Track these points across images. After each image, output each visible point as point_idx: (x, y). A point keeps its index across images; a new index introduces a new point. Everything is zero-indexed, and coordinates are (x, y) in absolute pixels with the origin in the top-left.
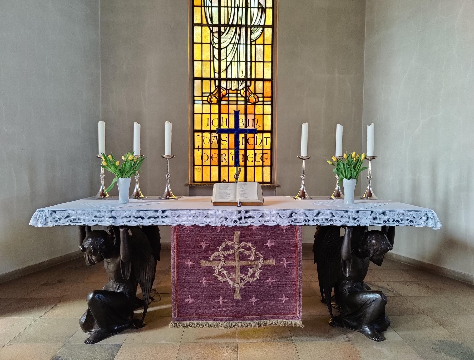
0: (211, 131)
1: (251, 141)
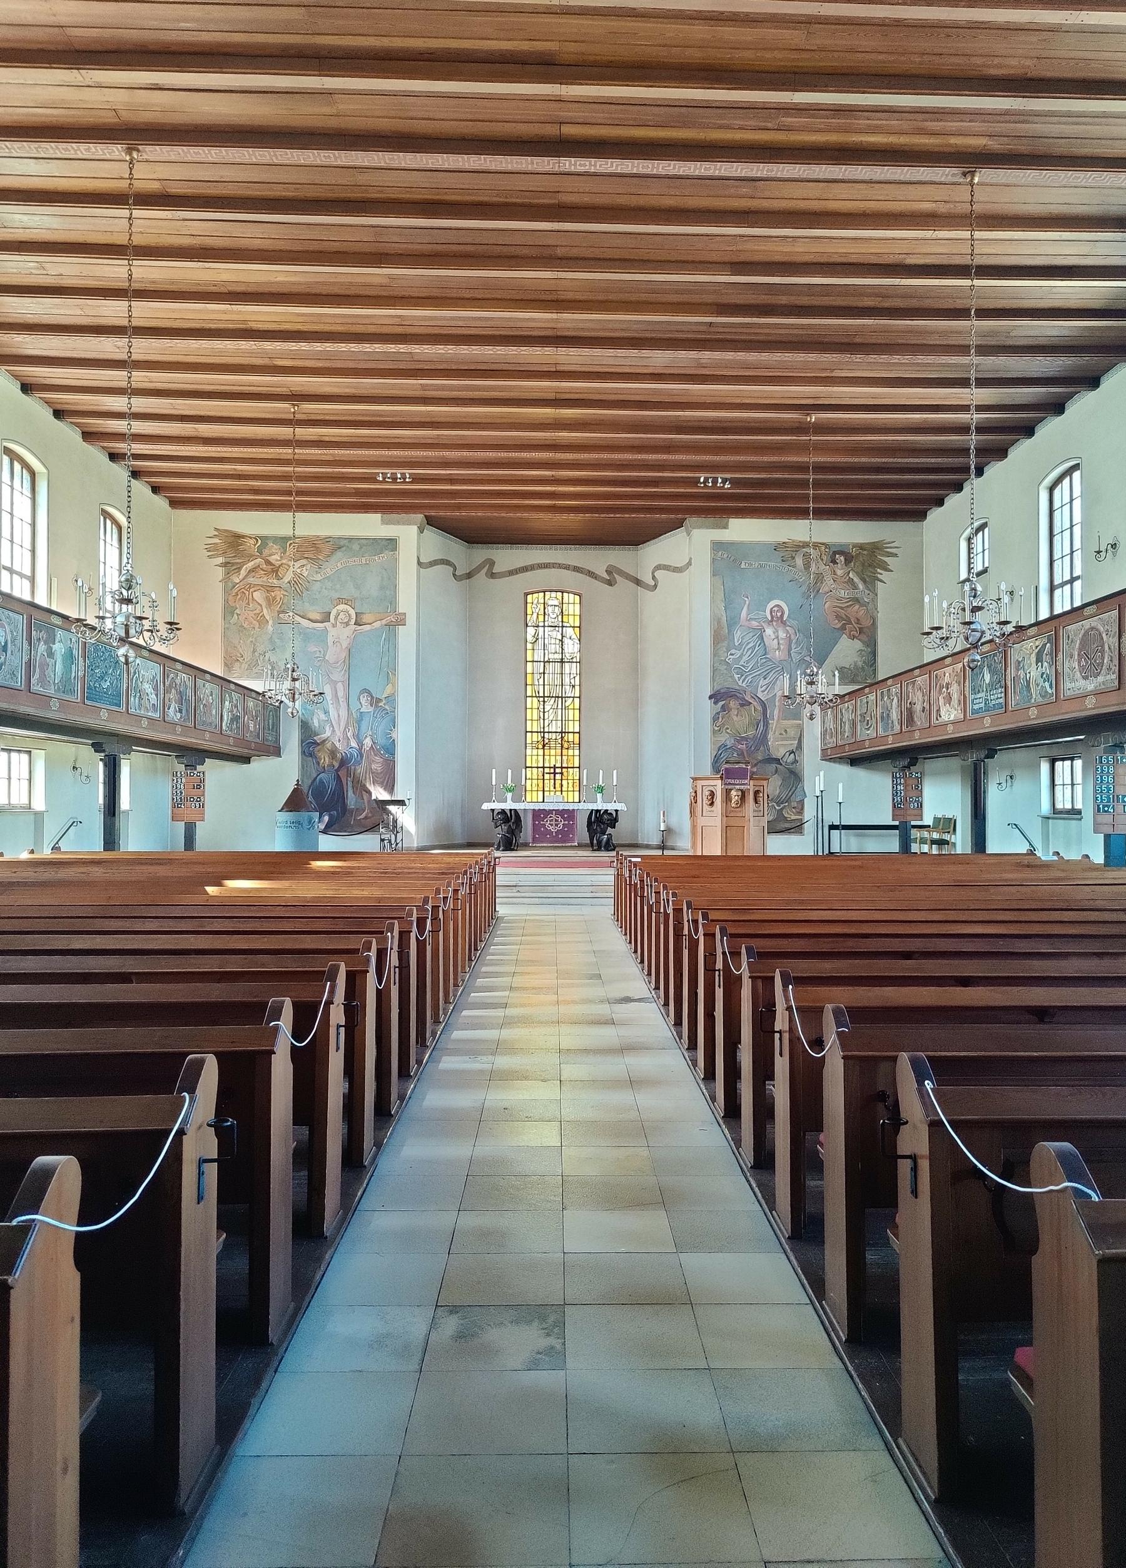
0: (538, 768)
1: (565, 774)
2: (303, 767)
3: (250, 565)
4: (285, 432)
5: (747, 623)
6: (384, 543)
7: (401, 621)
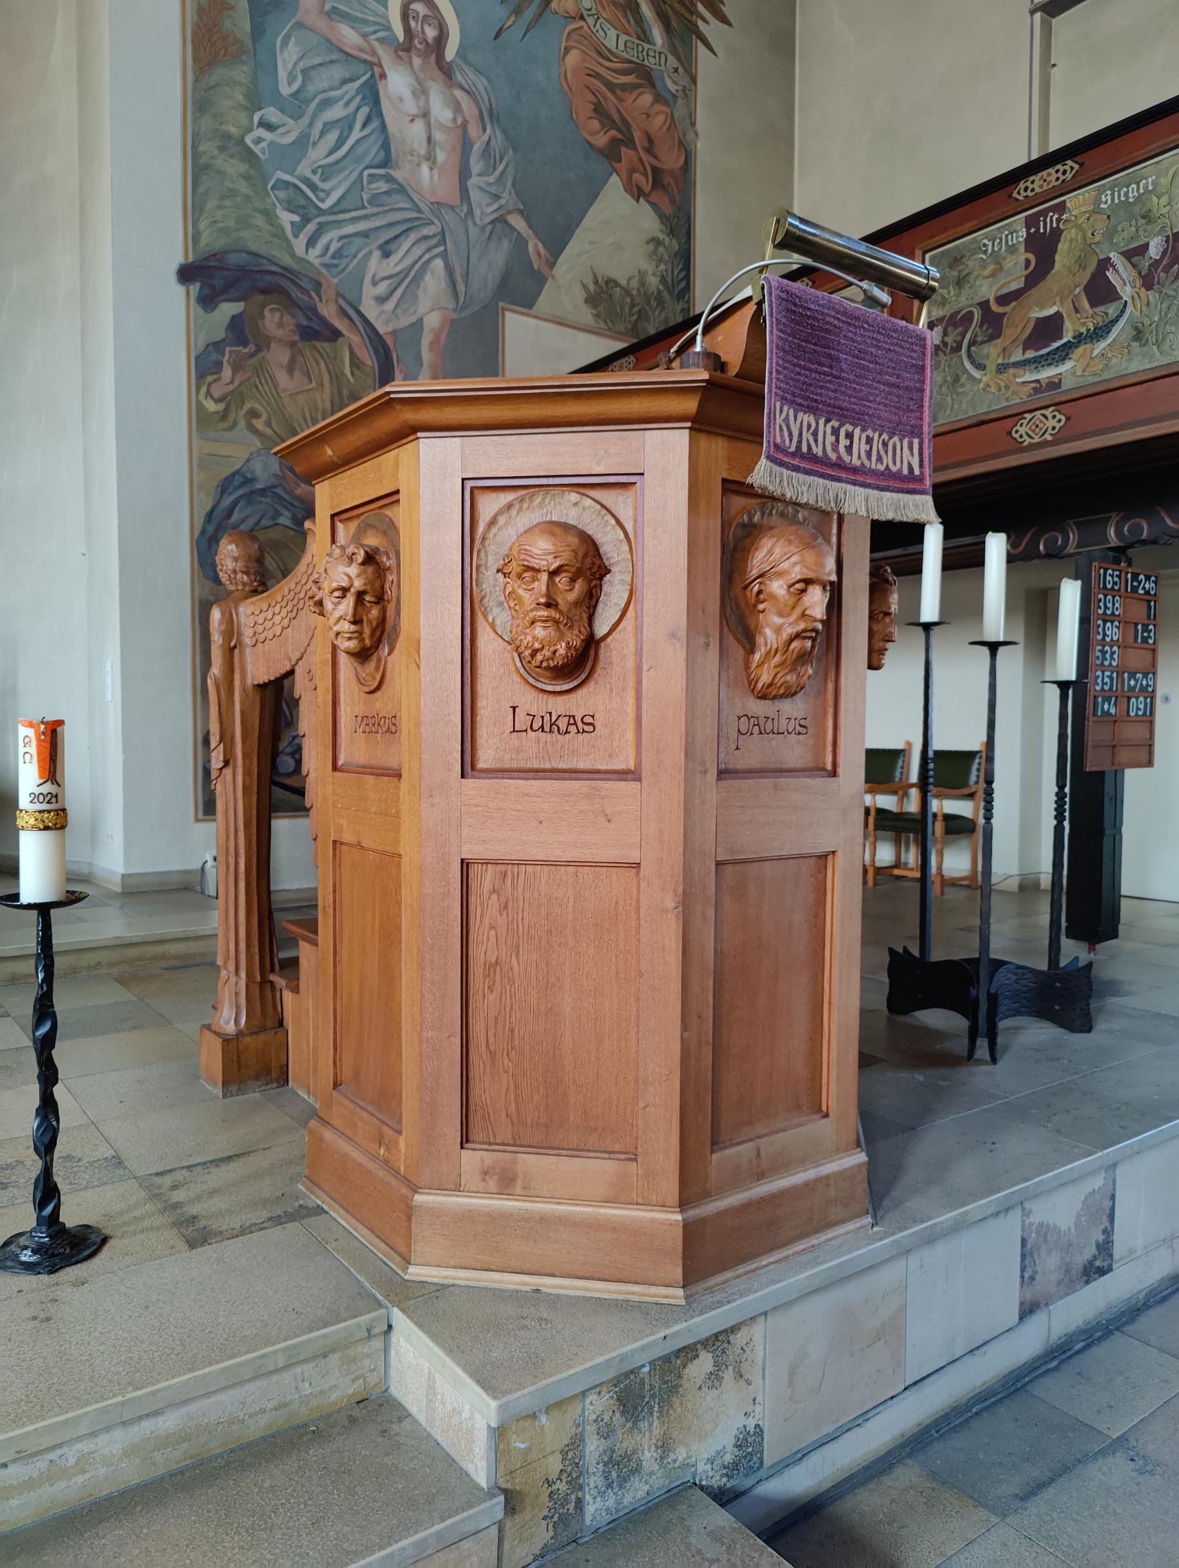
5: (322, 24)
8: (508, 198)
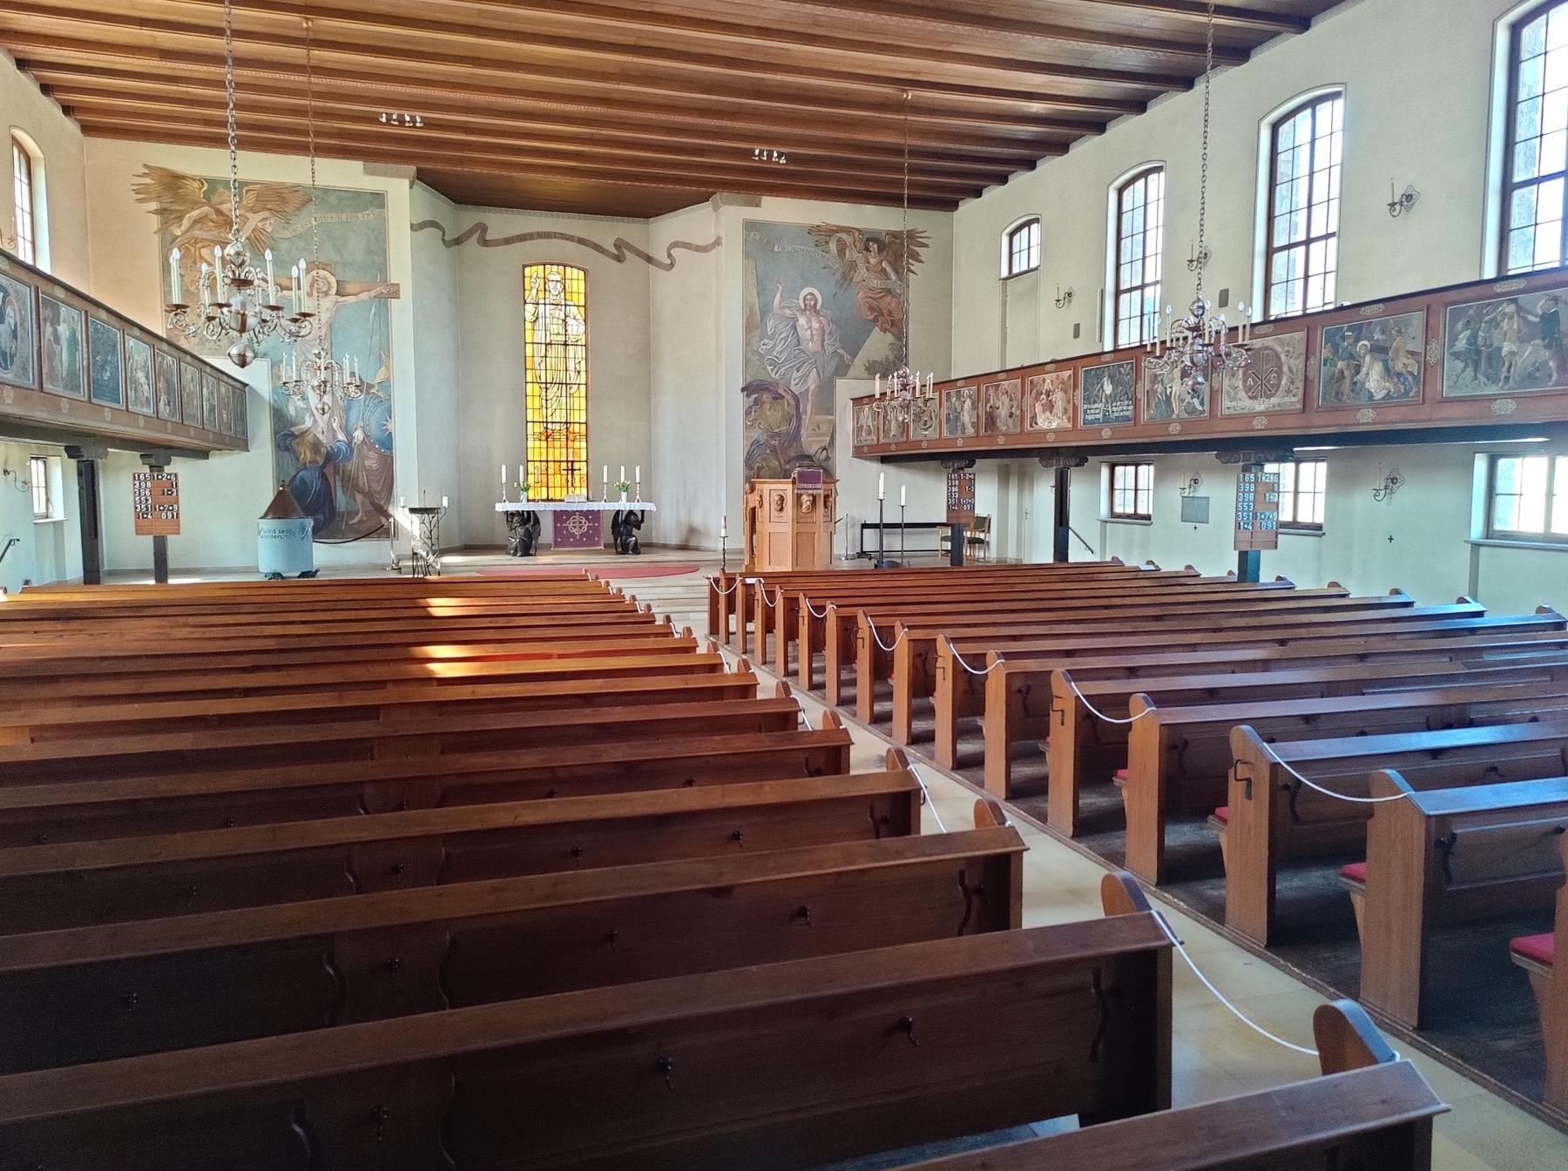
0: (541, 461)
2: (279, 466)
3: (195, 214)
4: (296, 53)
6: (368, 197)
7: (394, 292)
8: (837, 344)
